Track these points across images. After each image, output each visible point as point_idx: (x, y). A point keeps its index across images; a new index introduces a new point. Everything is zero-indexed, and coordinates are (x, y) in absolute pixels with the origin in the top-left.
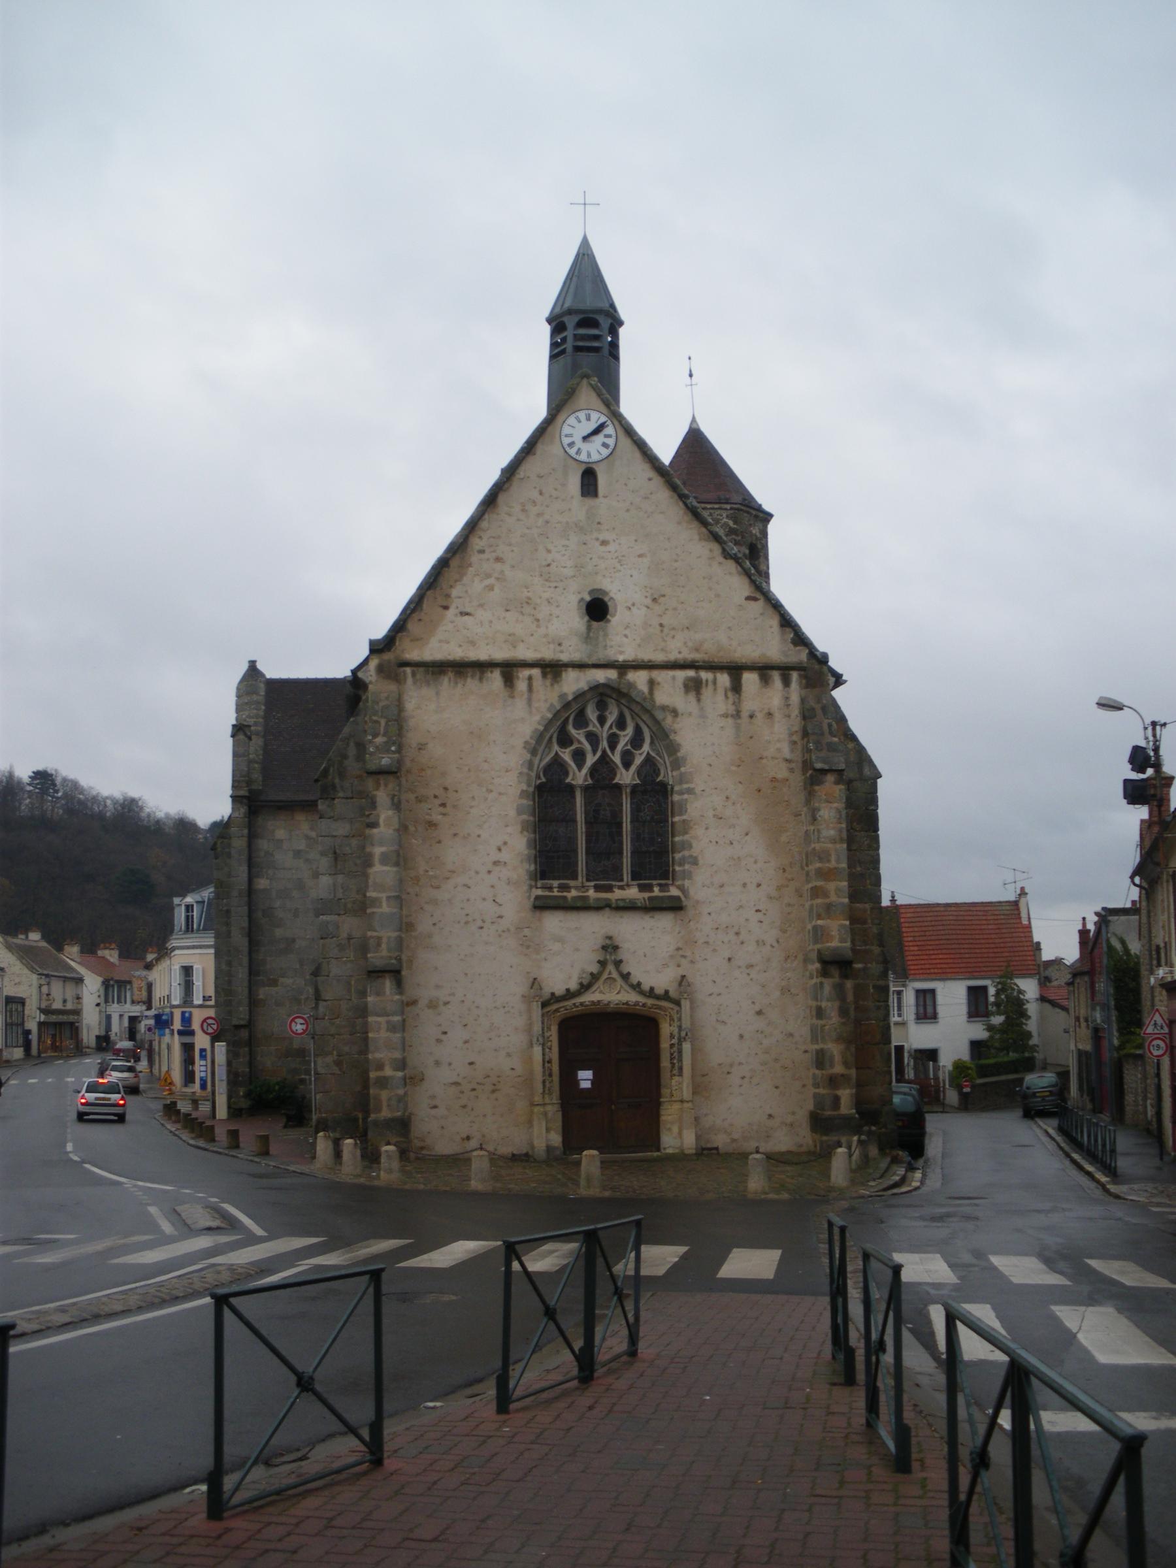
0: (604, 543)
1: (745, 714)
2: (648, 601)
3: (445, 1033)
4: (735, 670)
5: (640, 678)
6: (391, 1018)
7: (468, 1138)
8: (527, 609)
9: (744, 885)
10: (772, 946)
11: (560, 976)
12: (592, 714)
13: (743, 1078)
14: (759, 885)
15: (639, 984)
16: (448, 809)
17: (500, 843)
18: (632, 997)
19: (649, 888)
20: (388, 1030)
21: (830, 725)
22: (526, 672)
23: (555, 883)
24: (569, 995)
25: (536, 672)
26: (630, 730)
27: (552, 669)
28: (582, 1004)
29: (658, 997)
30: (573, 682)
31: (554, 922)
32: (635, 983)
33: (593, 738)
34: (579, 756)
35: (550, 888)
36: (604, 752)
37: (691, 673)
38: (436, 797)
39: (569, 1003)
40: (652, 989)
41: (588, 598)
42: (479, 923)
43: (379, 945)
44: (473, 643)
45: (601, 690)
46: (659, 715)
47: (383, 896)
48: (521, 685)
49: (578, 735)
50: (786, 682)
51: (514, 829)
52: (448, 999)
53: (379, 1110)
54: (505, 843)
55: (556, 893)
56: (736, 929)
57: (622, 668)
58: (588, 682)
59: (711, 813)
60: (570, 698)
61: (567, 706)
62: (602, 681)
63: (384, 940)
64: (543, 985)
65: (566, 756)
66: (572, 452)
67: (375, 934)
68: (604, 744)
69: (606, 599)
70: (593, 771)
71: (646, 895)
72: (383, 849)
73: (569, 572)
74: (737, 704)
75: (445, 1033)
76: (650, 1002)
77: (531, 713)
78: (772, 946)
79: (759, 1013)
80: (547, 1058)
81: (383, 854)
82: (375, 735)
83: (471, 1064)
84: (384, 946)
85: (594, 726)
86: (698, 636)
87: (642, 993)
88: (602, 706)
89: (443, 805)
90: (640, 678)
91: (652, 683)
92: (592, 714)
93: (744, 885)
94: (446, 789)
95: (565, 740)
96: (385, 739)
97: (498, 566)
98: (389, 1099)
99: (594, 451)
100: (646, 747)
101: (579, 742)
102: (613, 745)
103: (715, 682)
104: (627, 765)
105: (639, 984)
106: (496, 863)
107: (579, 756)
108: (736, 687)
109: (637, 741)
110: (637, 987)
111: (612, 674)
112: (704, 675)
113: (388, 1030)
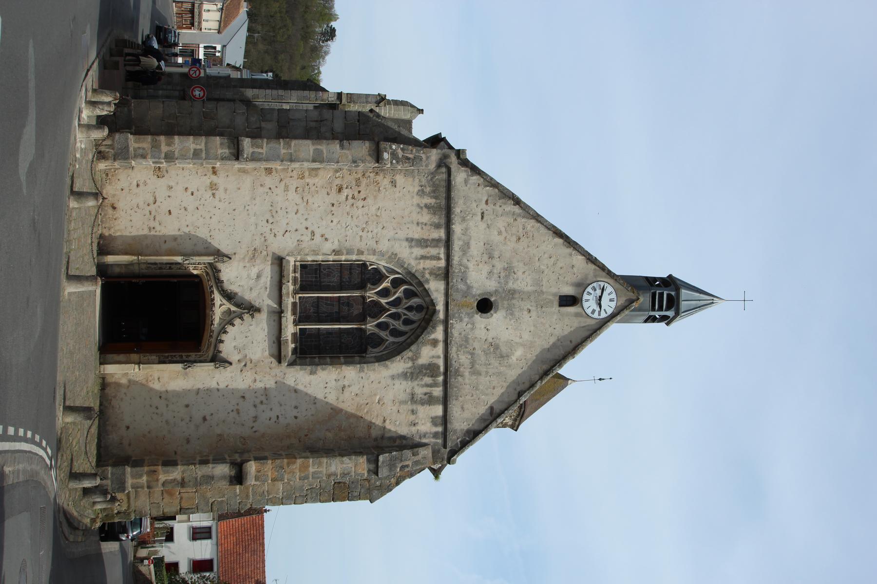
0: (529, 311)
1: (414, 407)
2: (490, 340)
3: (192, 194)
4: (445, 401)
5: (438, 333)
6: (204, 152)
7: (114, 208)
8: (486, 257)
9: (296, 407)
10: (252, 428)
11: (232, 274)
12: (415, 301)
13: (157, 408)
14: (296, 417)
15: (225, 332)
16: (351, 201)
17: (326, 236)
19: (294, 340)
20: (195, 150)
21: (407, 466)
22: (442, 256)
23: (298, 275)
24: (219, 282)
25: (442, 263)
26: (403, 328)
27: (446, 274)
28: (212, 292)
29: (216, 346)
30: (436, 288)
31: (268, 271)
32: (227, 330)
33: (396, 303)
34: (385, 293)
35: (295, 272)
36: (389, 310)
37: (442, 369)
38: (359, 192)
39: (212, 283)
40: (222, 341)
41: (492, 299)
42: (270, 222)
43: (258, 147)
44: (464, 219)
45: (430, 307)
46: (413, 348)
47: (292, 151)
48: (433, 251)
49: (399, 293)
52: (217, 196)
53: (135, 142)
54: (326, 239)
55: (292, 275)
56: (265, 401)
57: (446, 322)
58: (436, 298)
59: (346, 383)
60: (426, 286)
61: (421, 284)
62: (437, 308)
63: (260, 150)
64: (226, 264)
65: (385, 284)
66: (589, 289)
67: (265, 145)
68: (393, 310)
69: (492, 312)
70: (375, 304)
71: (290, 338)
72: (325, 151)
73: (511, 285)
74: (422, 403)
75: (192, 194)
76: (213, 340)
77: (416, 259)
78: (252, 428)
79: (205, 419)
80: (173, 266)
81: (322, 151)
82: (402, 149)
83: (170, 212)
84: (256, 150)
85: (406, 303)
86: (467, 374)
88: (419, 308)
89: (353, 198)
90: (438, 333)
91: (435, 343)
92: (415, 301)
93: (296, 407)
94: (364, 199)
95: (396, 283)
96: (400, 156)
97: (514, 238)
98: (144, 149)
99: (589, 303)
100: (391, 339)
101: (395, 293)
102: (393, 316)
103: (435, 385)
105: (225, 332)
106: (313, 233)
108: (430, 400)
109: (395, 333)
111: (441, 316)
112: (441, 379)
113: (195, 150)
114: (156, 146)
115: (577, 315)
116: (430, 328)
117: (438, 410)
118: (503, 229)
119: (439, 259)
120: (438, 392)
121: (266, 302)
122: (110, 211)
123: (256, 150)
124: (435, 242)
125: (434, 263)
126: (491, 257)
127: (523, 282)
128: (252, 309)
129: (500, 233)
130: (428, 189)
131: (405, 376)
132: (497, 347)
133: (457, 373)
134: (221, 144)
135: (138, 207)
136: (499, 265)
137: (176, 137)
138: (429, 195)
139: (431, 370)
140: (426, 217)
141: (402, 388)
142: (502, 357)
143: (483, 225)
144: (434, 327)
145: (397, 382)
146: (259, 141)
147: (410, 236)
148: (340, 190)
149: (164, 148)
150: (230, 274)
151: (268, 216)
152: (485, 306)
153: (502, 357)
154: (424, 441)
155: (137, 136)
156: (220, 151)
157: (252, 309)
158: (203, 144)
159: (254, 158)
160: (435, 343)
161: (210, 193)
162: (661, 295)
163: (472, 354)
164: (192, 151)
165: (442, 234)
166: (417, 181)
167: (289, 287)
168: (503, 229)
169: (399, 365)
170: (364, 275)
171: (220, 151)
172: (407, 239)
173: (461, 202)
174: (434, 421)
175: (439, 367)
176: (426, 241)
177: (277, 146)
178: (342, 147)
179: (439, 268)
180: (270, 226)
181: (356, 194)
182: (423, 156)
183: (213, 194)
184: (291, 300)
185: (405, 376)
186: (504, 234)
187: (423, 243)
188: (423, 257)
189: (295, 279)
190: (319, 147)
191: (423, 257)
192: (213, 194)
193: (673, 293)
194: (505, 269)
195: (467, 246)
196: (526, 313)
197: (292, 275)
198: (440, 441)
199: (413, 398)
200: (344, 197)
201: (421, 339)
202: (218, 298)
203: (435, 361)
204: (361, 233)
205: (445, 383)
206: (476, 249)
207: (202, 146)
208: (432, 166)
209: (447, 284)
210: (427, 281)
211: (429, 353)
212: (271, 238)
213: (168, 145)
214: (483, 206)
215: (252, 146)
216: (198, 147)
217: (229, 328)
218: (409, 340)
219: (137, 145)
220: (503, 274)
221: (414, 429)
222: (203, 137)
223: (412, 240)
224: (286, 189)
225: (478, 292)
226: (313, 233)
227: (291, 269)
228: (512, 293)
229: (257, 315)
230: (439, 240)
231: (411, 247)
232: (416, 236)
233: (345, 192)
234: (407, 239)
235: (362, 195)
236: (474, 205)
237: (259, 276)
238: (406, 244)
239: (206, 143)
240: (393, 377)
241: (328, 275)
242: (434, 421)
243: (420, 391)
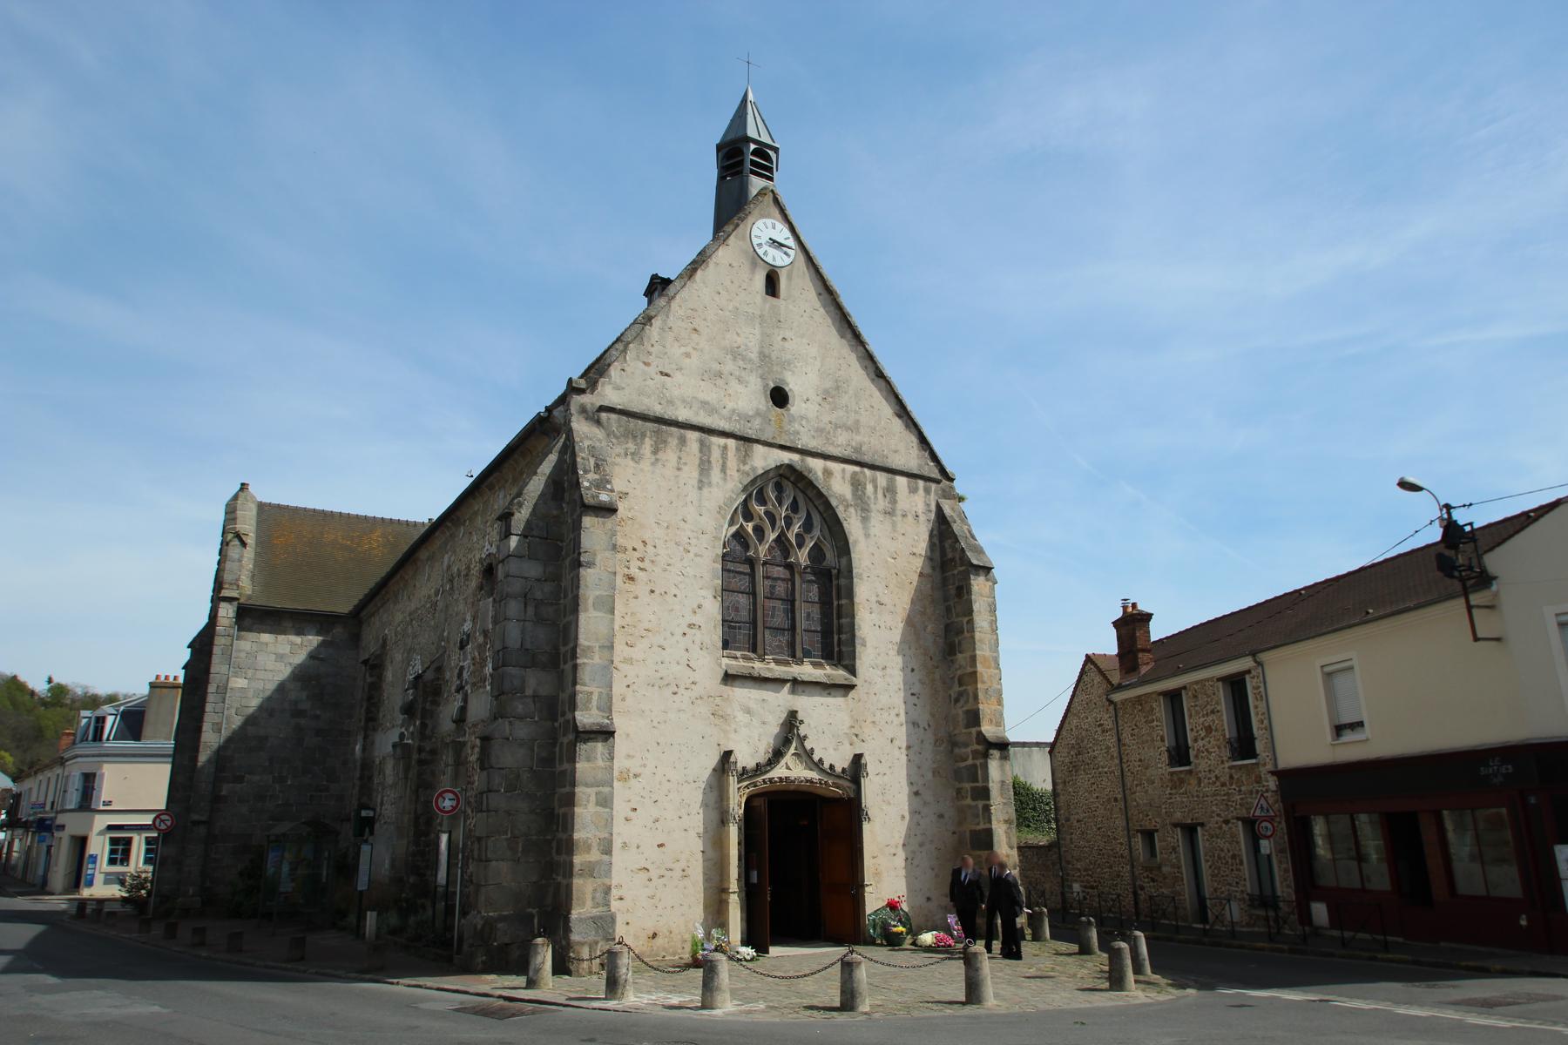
1: (899, 513)
2: (819, 399)
8: (720, 382)
12: (771, 494)
16: (646, 564)
18: (814, 775)
20: (598, 804)
22: (722, 441)
23: (738, 654)
24: (759, 769)
25: (731, 443)
26: (803, 514)
28: (771, 780)
29: (838, 777)
30: (765, 459)
31: (743, 694)
34: (759, 531)
37: (857, 469)
43: (589, 701)
44: (671, 402)
46: (834, 503)
48: (716, 454)
50: (927, 491)
51: (709, 594)
53: (583, 905)
57: (804, 452)
59: (874, 599)
60: (760, 472)
61: (753, 482)
63: (595, 697)
65: (749, 527)
66: (761, 252)
73: (754, 356)
74: (894, 502)
82: (586, 472)
84: (594, 703)
86: (858, 438)
87: (823, 771)
88: (779, 488)
89: (642, 560)
90: (816, 465)
92: (771, 494)
95: (748, 516)
97: (695, 336)
99: (777, 258)
100: (816, 532)
103: (874, 481)
104: (800, 546)
106: (691, 626)
107: (759, 531)
108: (890, 490)
109: (808, 526)
110: (818, 765)
111: (796, 457)
114: (590, 871)
115: (789, 277)
116: (810, 476)
117: (901, 481)
118: (683, 350)
119: (725, 447)
120: (882, 478)
121: (780, 701)
122: (659, 941)
123: (594, 703)
124: (704, 448)
125: (731, 453)
126: (720, 375)
127: (749, 338)
128: (791, 722)
129: (688, 355)
130: (631, 446)
131: (865, 520)
132: (826, 392)
133: (858, 450)
134: (588, 760)
135: (652, 897)
136: (729, 366)
137: (576, 836)
138: (639, 446)
139: (857, 484)
140: (670, 455)
141: (878, 524)
142: (838, 388)
143: (678, 377)
144: (810, 471)
145: (873, 531)
146: (579, 697)
147: (695, 482)
148: (631, 579)
149: (595, 855)
150: (746, 757)
151: (668, 692)
152: (779, 397)
153: (838, 388)
154: (933, 508)
155: (574, 902)
156: (600, 763)
157: (791, 722)
158: (589, 790)
159: (608, 708)
160: (828, 473)
161: (633, 782)
162: (753, 163)
163: (837, 427)
164: (599, 809)
165: (693, 436)
166: (618, 460)
167: (758, 667)
168: (683, 350)
169: (852, 526)
170: (738, 558)
171: (600, 763)
172: (700, 488)
173: (646, 401)
174: (913, 490)
175: (855, 473)
176: (702, 462)
177: (588, 668)
178: (590, 564)
179: (738, 449)
180: (681, 690)
181: (637, 555)
182: (587, 443)
183: (636, 776)
184: (773, 665)
185: (865, 520)
186: (689, 349)
187: (704, 466)
188: (724, 469)
189: (745, 658)
190: (590, 601)
191: (724, 469)
192: (636, 776)
193: (753, 146)
194: (735, 359)
195: (704, 404)
196: (786, 344)
197: (742, 663)
198: (933, 486)
199: (890, 513)
200: (642, 574)
201: (823, 491)
202: (778, 772)
203: (848, 476)
204: (691, 555)
205: (873, 467)
206: (709, 394)
207: (592, 791)
208: (598, 433)
209: (757, 441)
210: (754, 469)
211: (837, 483)
212: (697, 690)
213: (588, 849)
214: (652, 370)
215: (588, 709)
216: (593, 798)
217: (816, 758)
218: (821, 508)
219: (589, 903)
220: (741, 363)
221: (922, 518)
222: (577, 790)
223: (700, 481)
224: (629, 661)
225: (763, 401)
226: (691, 626)
227: (734, 662)
228: (764, 356)
229: (800, 716)
230: (702, 443)
231: (710, 484)
232: (695, 474)
233: (634, 571)
234: (700, 488)
235: (639, 546)
236: (650, 382)
237: (748, 711)
238: (705, 490)
239: (587, 785)
240: (867, 536)
241: (737, 610)
242: (913, 490)
243: (882, 503)
